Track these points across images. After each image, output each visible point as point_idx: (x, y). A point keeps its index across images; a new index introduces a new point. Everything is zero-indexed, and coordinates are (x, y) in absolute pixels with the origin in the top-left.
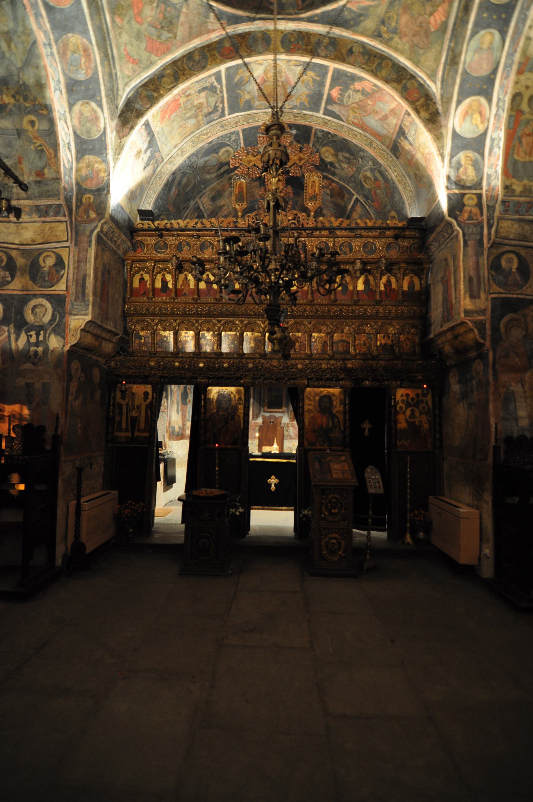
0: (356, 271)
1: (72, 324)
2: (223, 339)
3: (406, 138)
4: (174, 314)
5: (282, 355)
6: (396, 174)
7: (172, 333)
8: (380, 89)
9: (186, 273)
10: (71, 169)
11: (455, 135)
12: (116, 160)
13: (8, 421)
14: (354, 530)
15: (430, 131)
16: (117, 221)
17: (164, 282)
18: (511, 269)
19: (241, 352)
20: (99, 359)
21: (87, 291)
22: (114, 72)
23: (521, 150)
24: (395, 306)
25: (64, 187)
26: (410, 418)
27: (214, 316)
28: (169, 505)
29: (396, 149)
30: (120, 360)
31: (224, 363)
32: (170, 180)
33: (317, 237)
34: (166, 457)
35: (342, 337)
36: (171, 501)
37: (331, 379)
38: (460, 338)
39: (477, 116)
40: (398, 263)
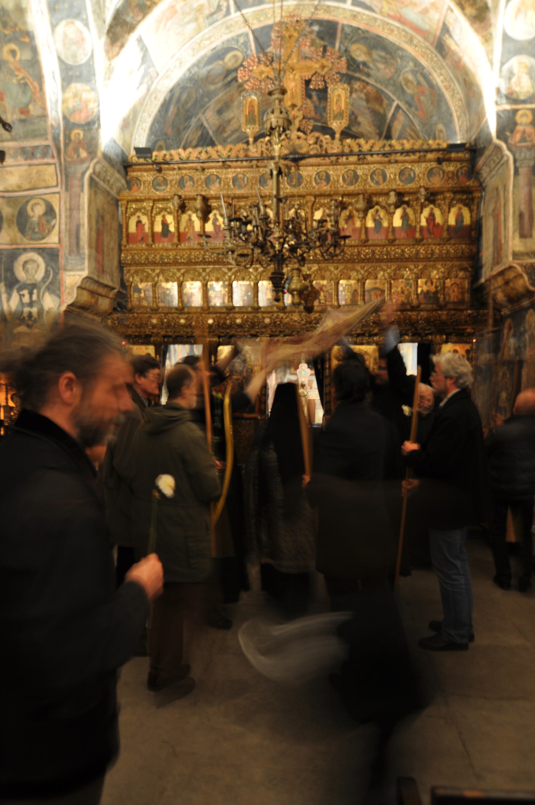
0: (389, 205)
2: (235, 290)
3: (451, 36)
4: (177, 262)
5: (305, 308)
6: (442, 78)
10: (57, 101)
17: (165, 225)
19: (256, 305)
24: (439, 245)
29: (441, 47)
30: (118, 318)
32: (167, 99)
33: (344, 164)
37: (363, 335)
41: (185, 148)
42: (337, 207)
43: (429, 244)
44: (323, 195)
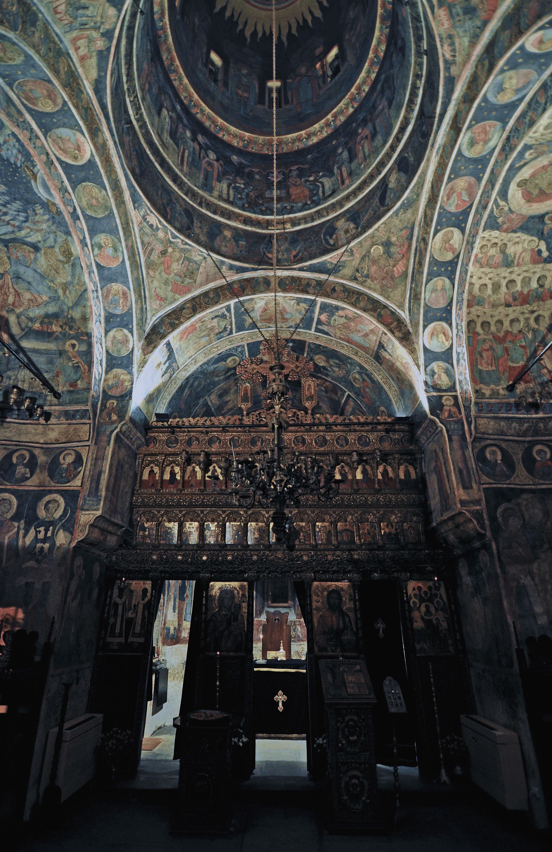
0: (353, 462)
5: (287, 546)
8: (360, 316)
9: (194, 465)
14: (378, 765)
15: (404, 346)
18: (496, 460)
23: (483, 362)
26: (425, 615)
28: (158, 734)
31: (227, 555)
34: (158, 667)
35: (346, 526)
36: (160, 728)
38: (461, 528)
39: (441, 336)
40: (392, 454)
41: (194, 418)
42: (312, 462)
44: (301, 454)
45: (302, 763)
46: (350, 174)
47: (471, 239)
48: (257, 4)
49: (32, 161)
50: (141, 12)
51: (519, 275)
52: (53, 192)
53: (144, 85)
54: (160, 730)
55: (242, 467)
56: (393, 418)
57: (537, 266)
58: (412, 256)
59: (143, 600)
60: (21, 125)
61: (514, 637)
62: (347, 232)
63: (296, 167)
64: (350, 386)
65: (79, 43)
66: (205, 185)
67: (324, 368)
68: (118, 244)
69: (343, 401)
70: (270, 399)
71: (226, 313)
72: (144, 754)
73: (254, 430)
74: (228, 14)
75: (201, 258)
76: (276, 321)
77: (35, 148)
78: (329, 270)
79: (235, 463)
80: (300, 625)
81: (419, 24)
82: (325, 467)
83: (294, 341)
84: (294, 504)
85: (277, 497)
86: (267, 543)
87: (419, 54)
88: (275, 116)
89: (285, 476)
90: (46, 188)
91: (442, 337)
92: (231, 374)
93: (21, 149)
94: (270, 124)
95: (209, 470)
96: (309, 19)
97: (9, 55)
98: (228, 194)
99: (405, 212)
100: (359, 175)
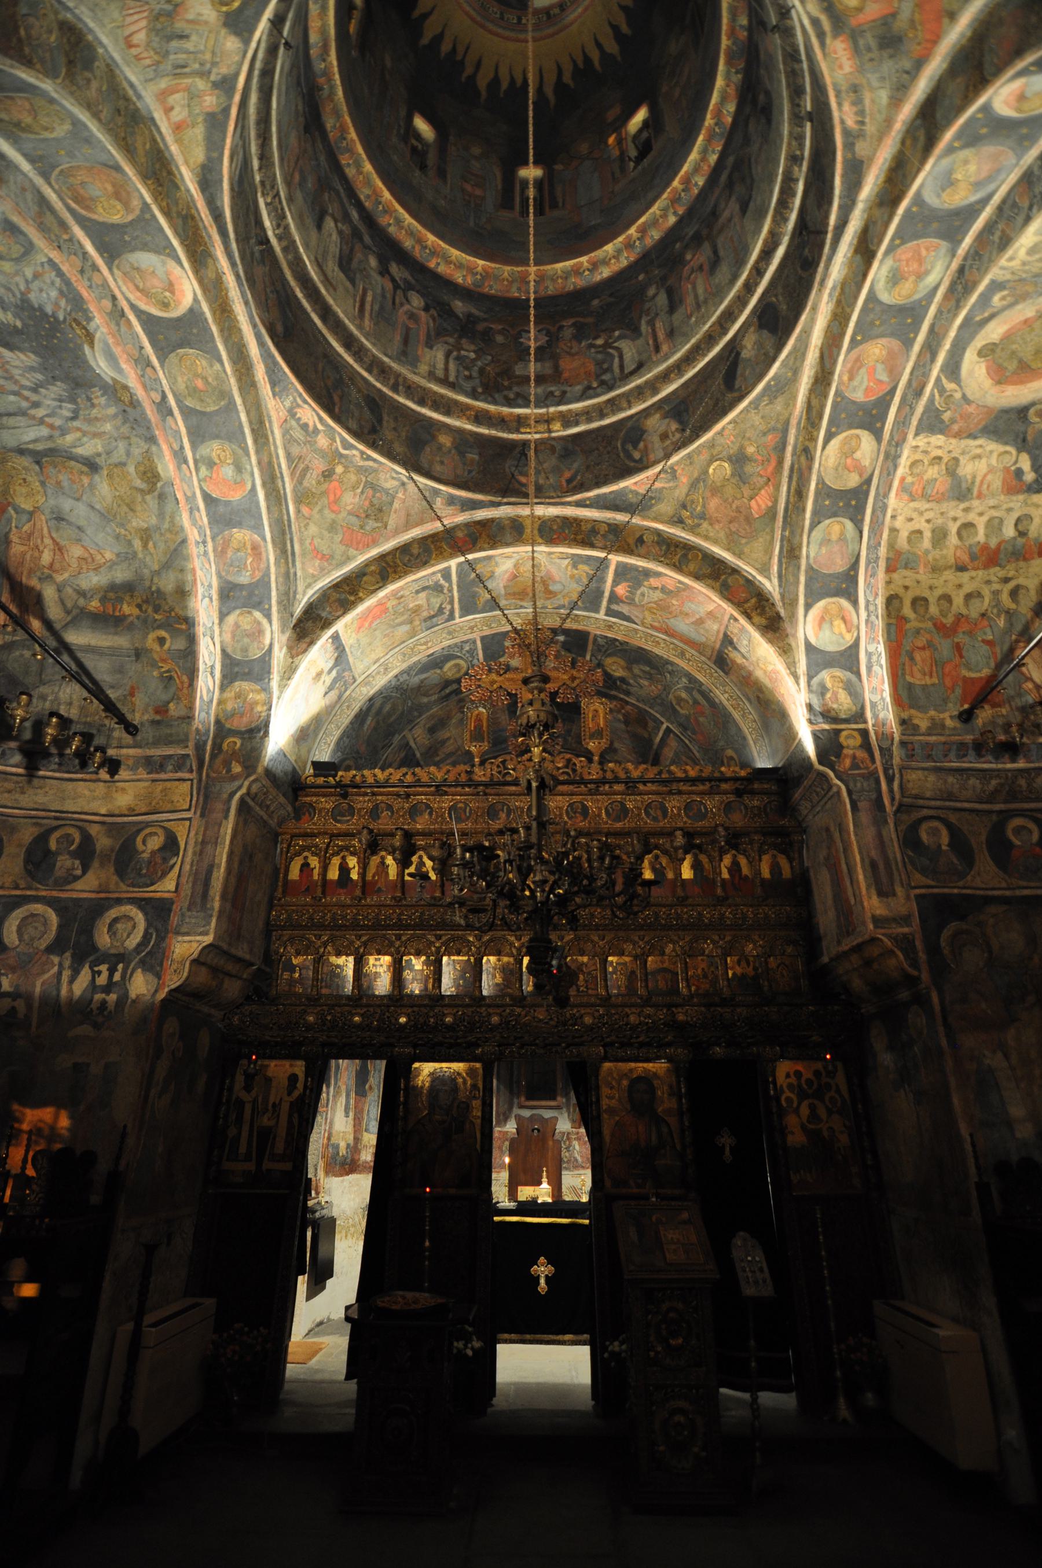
0: (676, 849)
1: (177, 951)
2: (445, 969)
4: (358, 925)
5: (554, 999)
7: (351, 959)
9: (383, 853)
10: (211, 701)
11: (809, 647)
12: (283, 687)
13: (25, 1142)
14: (723, 1390)
16: (274, 776)
17: (344, 870)
18: (940, 846)
20: (213, 1011)
21: (211, 893)
22: (292, 571)
23: (915, 669)
25: (197, 730)
27: (430, 928)
28: (317, 1335)
31: (445, 1015)
34: (317, 1215)
35: (662, 962)
36: (321, 1323)
37: (648, 1044)
38: (875, 966)
42: (600, 849)
43: (736, 905)
44: (580, 833)
45: (583, 1386)
46: (671, 334)
47: (893, 449)
48: (500, 31)
49: (86, 312)
50: (286, 44)
51: (981, 514)
52: (124, 366)
53: (292, 176)
54: (320, 1326)
55: (472, 857)
56: (749, 770)
57: (1014, 498)
58: (785, 480)
59: (289, 1094)
60: (64, 247)
61: (972, 1160)
62: (664, 436)
63: (571, 321)
64: (670, 711)
65: (172, 100)
66: (404, 353)
67: (623, 680)
68: (244, 459)
69: (658, 739)
70: (524, 735)
71: (442, 582)
72: (291, 1370)
73: (493, 791)
74: (445, 47)
75: (396, 483)
76: (534, 596)
77: (90, 287)
78: (631, 505)
79: (458, 851)
80: (578, 1139)
81: (796, 66)
82: (624, 857)
83: (566, 632)
84: (568, 923)
85: (535, 911)
86: (517, 993)
87: (797, 119)
88: (531, 230)
89: (552, 873)
90: (111, 358)
91: (839, 626)
92: (451, 691)
93: (65, 289)
94: (525, 245)
95: (411, 863)
96: (595, 56)
97: (44, 121)
98: (446, 369)
99: (771, 402)
100: (687, 337)
